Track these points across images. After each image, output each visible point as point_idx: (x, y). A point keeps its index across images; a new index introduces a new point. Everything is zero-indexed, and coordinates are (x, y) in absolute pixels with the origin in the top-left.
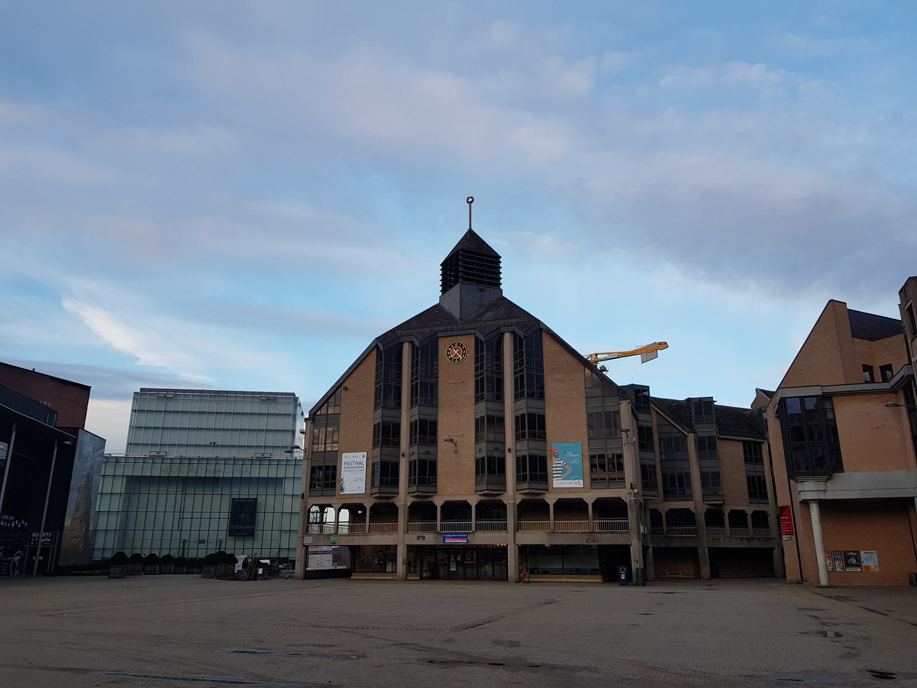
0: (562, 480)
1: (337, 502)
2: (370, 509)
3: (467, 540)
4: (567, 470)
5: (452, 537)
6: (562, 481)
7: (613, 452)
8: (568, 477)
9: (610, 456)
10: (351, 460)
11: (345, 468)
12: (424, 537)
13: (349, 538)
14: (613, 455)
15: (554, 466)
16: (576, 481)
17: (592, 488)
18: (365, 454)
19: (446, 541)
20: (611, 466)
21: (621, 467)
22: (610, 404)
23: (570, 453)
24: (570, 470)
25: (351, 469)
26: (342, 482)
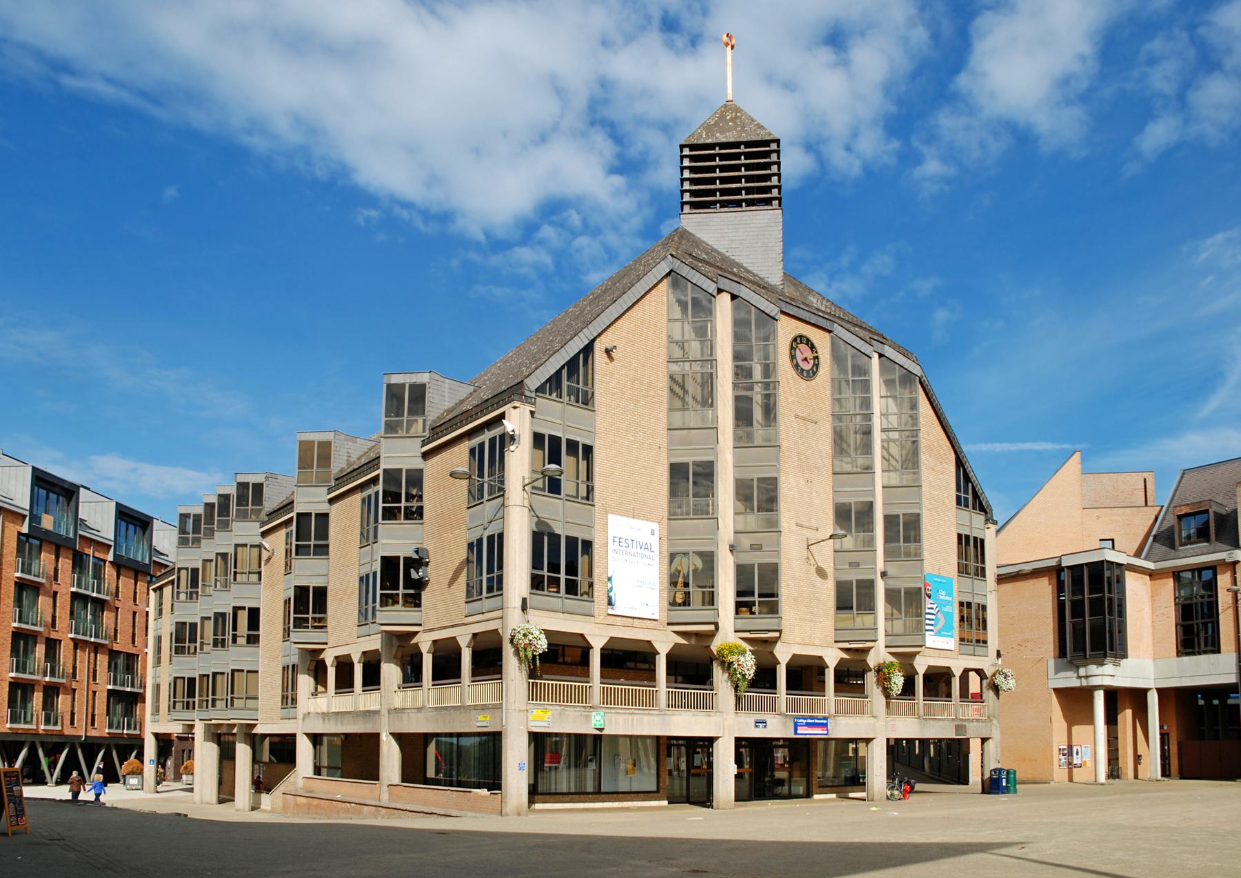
0: (935, 635)
1: (597, 632)
5: (808, 725)
8: (940, 632)
12: (765, 723)
13: (630, 717)
17: (961, 652)
18: (656, 526)
19: (799, 732)
21: (984, 624)
26: (609, 585)
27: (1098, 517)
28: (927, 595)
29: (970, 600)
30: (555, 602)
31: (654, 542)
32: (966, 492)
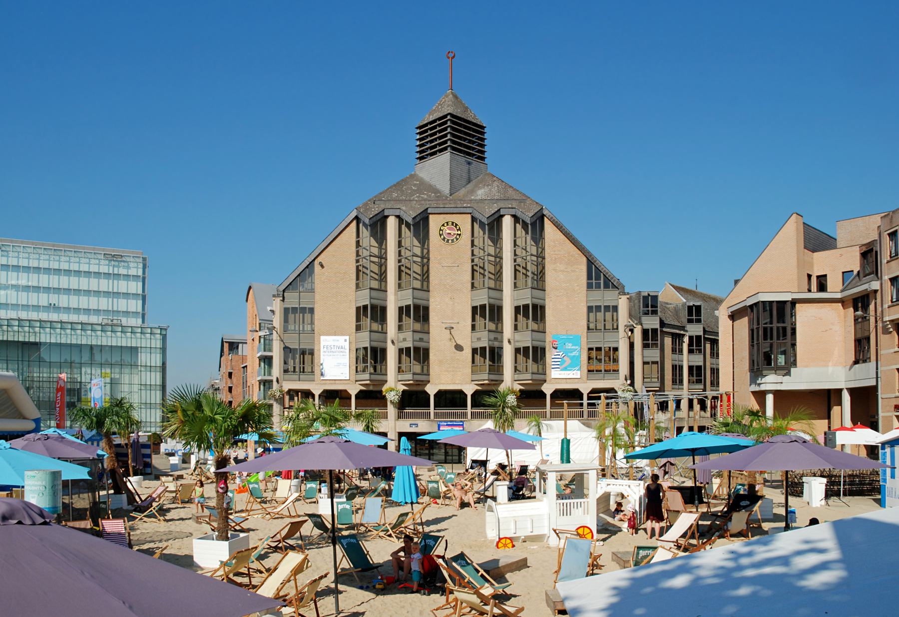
0: (561, 370)
2: (356, 395)
3: (463, 428)
4: (565, 361)
5: (447, 425)
6: (561, 372)
7: (610, 345)
9: (607, 349)
10: (332, 343)
11: (325, 352)
14: (610, 348)
15: (553, 357)
16: (574, 372)
18: (347, 338)
20: (607, 359)
21: (616, 361)
22: (607, 297)
23: (569, 345)
24: (568, 361)
25: (331, 354)
26: (321, 367)
27: (841, 255)
28: (553, 347)
29: (598, 346)
30: (296, 377)
31: (347, 344)
32: (598, 278)
